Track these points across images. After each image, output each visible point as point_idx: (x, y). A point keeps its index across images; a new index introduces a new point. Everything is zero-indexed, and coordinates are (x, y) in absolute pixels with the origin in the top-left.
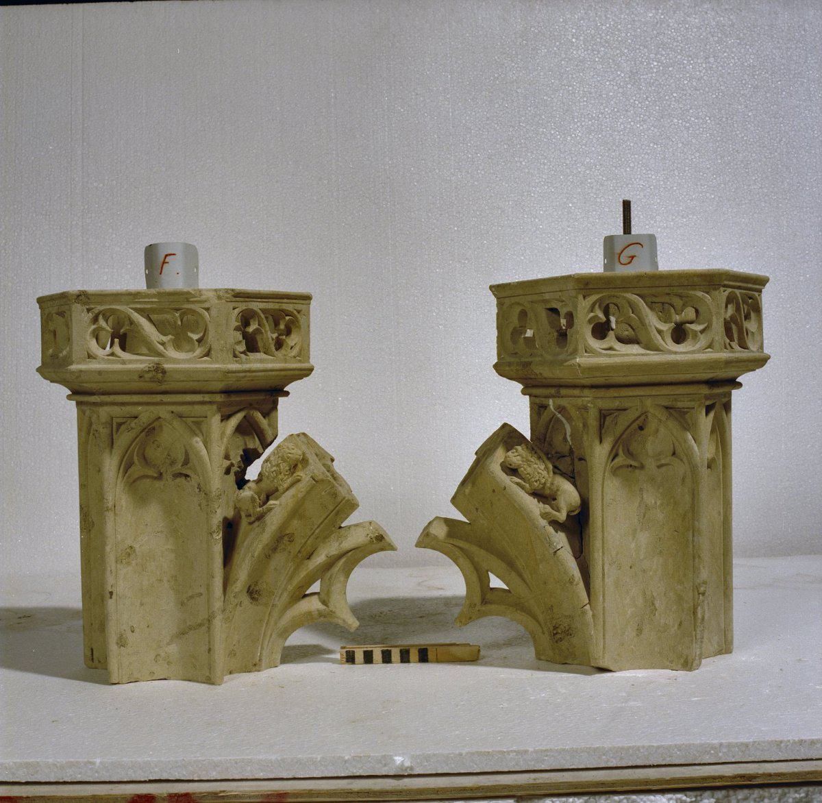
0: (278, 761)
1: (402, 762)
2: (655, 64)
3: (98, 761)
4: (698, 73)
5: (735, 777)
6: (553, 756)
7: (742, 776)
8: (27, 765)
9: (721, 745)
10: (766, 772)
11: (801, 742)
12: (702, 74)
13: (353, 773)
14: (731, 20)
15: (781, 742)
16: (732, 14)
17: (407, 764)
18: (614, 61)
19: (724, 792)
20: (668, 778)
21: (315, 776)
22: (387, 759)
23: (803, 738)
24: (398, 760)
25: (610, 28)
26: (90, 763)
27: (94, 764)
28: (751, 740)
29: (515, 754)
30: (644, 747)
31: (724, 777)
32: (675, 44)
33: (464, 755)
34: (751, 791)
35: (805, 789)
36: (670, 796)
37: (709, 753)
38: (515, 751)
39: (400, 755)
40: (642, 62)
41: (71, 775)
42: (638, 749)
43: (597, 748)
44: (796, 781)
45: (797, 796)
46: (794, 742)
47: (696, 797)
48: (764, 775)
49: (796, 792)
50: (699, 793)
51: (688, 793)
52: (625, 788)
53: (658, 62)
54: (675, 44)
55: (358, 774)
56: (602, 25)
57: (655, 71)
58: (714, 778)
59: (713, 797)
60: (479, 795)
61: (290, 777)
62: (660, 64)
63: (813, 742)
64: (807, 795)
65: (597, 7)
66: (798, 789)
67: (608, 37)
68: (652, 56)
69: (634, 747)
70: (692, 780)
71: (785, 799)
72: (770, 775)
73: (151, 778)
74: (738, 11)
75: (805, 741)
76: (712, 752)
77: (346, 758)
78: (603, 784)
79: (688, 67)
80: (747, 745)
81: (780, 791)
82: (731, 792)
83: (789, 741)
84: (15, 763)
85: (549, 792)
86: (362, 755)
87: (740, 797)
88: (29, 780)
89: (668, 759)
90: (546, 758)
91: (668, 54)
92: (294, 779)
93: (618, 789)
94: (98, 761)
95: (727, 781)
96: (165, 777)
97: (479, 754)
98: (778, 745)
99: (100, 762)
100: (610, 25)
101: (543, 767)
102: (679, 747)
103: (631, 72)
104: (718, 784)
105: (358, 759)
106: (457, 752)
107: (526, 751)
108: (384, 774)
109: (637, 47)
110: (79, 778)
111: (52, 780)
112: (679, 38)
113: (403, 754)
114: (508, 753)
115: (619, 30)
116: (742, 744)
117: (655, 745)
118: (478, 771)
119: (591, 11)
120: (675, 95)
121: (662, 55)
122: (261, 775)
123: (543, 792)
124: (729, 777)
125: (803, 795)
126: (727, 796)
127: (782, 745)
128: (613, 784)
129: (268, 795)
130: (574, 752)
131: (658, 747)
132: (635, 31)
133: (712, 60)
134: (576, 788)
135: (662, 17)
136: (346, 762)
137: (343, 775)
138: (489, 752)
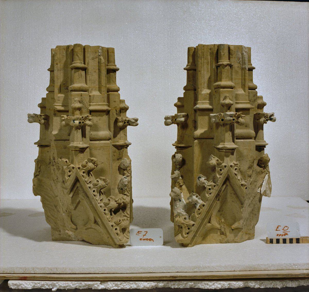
5: (171, 277)
7: (172, 277)
10: (181, 275)
19: (166, 282)
20: (148, 276)
31: (167, 277)
34: (175, 282)
35: (193, 282)
36: (148, 282)
44: (190, 279)
45: (190, 283)
47: (157, 283)
48: (180, 276)
49: (190, 283)
50: (158, 282)
51: (155, 282)
52: (135, 279)
58: (163, 277)
59: (163, 283)
60: (87, 280)
64: (194, 284)
66: (191, 282)
70: (156, 277)
71: (187, 285)
72: (182, 277)
78: (127, 278)
81: (185, 282)
82: (169, 282)
85: (110, 280)
87: (172, 284)
93: (132, 279)
95: (168, 278)
104: (165, 279)
123: (108, 280)
124: (169, 277)
125: (193, 283)
126: (168, 283)
128: (131, 278)
129: (21, 277)
134: (119, 279)
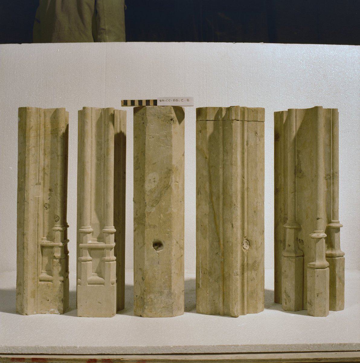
3: (78, 346)
8: (52, 347)
9: (311, 345)
11: (340, 344)
13: (174, 352)
15: (333, 344)
18: (317, 70)
23: (341, 343)
26: (75, 347)
27: (76, 347)
38: (234, 345)
40: (328, 71)
41: (68, 352)
42: (280, 345)
43: (265, 345)
46: (338, 344)
53: (335, 71)
61: (150, 353)
62: (335, 72)
63: (345, 345)
68: (333, 69)
73: (98, 353)
76: (307, 347)
77: (171, 347)
79: (347, 73)
80: (320, 345)
83: (336, 344)
86: (177, 346)
89: (291, 350)
94: (78, 346)
96: (103, 353)
98: (332, 345)
99: (79, 347)
102: (295, 345)
103: (324, 75)
105: (176, 347)
106: (213, 345)
107: (238, 346)
109: (326, 65)
110: (71, 353)
111: (61, 353)
114: (232, 346)
115: (319, 58)
116: (318, 345)
122: (140, 353)
127: (333, 345)
130: (256, 346)
131: (288, 345)
136: (171, 348)
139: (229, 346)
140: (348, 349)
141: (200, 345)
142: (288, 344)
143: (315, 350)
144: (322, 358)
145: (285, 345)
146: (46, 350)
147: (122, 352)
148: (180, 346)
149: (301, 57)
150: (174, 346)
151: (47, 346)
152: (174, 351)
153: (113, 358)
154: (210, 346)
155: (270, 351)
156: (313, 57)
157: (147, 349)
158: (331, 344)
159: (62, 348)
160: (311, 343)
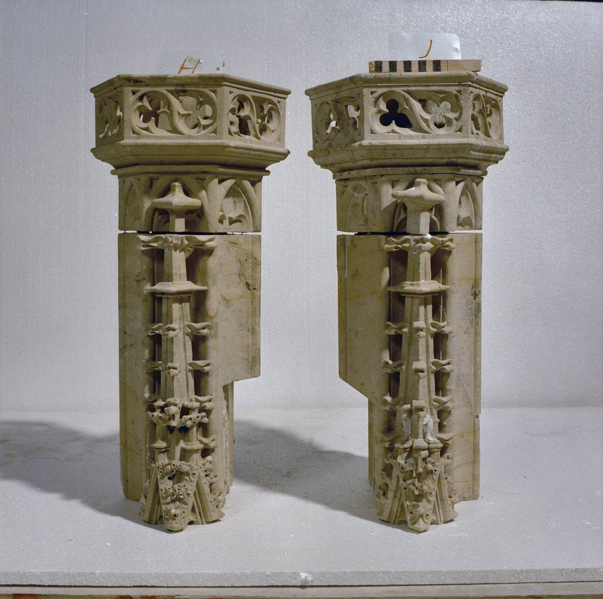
0: (222, 575)
1: (306, 577)
2: (500, 50)
3: (98, 572)
4: (531, 58)
6: (408, 576)
8: (50, 574)
9: (523, 571)
11: (576, 570)
12: (534, 59)
14: (556, 19)
15: (563, 570)
16: (557, 15)
17: (310, 578)
21: (246, 585)
22: (295, 575)
24: (303, 575)
25: (468, 23)
26: (93, 573)
27: (95, 574)
28: (543, 568)
29: (382, 573)
30: (470, 571)
32: (515, 36)
33: (348, 573)
37: (514, 576)
38: (382, 572)
39: (304, 572)
43: (438, 571)
46: (572, 570)
53: (502, 49)
54: (515, 36)
55: (276, 584)
56: (463, 21)
57: (500, 55)
62: (504, 51)
63: (584, 570)
65: (460, 8)
67: (467, 30)
69: (462, 572)
73: (135, 585)
74: (562, 13)
75: (579, 570)
76: (516, 575)
77: (268, 573)
80: (539, 571)
83: (568, 569)
84: (41, 573)
86: (278, 571)
88: (51, 584)
89: (486, 580)
90: (404, 577)
91: (510, 44)
92: (232, 587)
94: (98, 572)
96: (144, 584)
97: (358, 573)
98: (561, 572)
99: (100, 573)
100: (469, 21)
101: (401, 583)
102: (493, 572)
105: (276, 574)
107: (390, 573)
108: (293, 584)
110: (85, 583)
112: (518, 32)
113: (307, 572)
114: (378, 573)
115: (475, 25)
116: (536, 571)
117: (477, 570)
118: (357, 584)
119: (455, 10)
120: (514, 74)
121: (506, 44)
122: (209, 584)
127: (564, 572)
131: (479, 572)
132: (487, 26)
133: (542, 48)
135: (507, 16)
136: (268, 576)
137: (265, 585)
138: (364, 572)
139: (374, 573)
140: (591, 578)
141: (321, 572)
142: (481, 569)
143: (530, 579)
144: (544, 595)
145: (476, 571)
146: (40, 580)
147: (177, 583)
148: (284, 573)
149: (441, 23)
150: (273, 574)
151: (41, 571)
152: (273, 582)
153: (161, 594)
154: (339, 572)
155: (448, 583)
156: (464, 23)
157: (224, 578)
158: (559, 569)
159: (69, 575)
160: (524, 569)
